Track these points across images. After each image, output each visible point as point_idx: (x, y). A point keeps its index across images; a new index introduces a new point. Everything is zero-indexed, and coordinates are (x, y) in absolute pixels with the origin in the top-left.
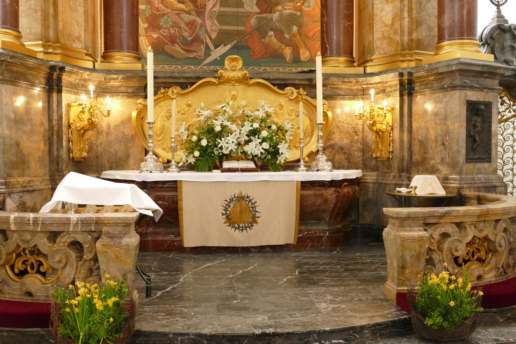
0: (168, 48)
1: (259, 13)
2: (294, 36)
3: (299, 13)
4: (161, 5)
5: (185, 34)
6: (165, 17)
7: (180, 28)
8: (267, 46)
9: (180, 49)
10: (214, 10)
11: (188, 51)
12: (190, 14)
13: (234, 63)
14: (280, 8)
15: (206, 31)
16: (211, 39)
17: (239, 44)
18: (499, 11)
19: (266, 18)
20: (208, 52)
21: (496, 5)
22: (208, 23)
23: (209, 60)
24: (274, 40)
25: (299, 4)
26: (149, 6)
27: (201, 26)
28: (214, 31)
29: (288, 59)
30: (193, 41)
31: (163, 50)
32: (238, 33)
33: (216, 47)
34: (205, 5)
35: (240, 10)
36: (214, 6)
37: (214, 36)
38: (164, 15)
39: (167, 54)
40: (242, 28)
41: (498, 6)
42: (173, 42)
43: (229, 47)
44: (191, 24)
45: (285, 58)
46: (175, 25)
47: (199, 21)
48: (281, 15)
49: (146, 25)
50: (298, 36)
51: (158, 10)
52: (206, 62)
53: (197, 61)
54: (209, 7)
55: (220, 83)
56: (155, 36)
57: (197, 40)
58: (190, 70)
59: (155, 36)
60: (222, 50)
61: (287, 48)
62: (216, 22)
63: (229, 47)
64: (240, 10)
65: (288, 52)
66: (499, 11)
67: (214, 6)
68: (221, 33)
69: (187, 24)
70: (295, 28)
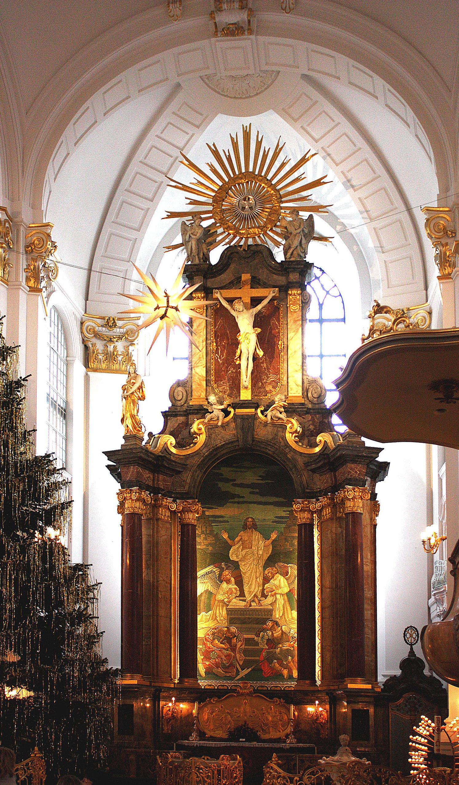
0: (215, 670)
1: (268, 649)
2: (289, 663)
3: (292, 649)
4: (211, 645)
5: (225, 662)
6: (213, 652)
7: (222, 659)
8: (273, 669)
9: (221, 671)
10: (241, 647)
11: (226, 672)
12: (227, 650)
13: (246, 685)
14: (281, 646)
15: (237, 660)
16: (239, 665)
17: (256, 668)
18: (412, 649)
19: (272, 652)
20: (238, 673)
21: (409, 645)
22: (238, 655)
23: (238, 677)
24: (277, 665)
25: (292, 643)
26: (204, 646)
27: (234, 657)
28: (241, 660)
29: (285, 677)
30: (229, 666)
31: (212, 671)
32: (256, 661)
33: (242, 670)
34: (236, 645)
35: (257, 647)
36: (241, 645)
37: (241, 663)
38: (213, 651)
39: (214, 674)
40: (258, 658)
41: (411, 645)
42: (218, 667)
43: (250, 669)
44: (227, 656)
45: (284, 677)
46: (219, 656)
47: (233, 654)
48: (281, 650)
49: (202, 657)
50: (292, 663)
51: (209, 648)
52: (236, 679)
53: (231, 678)
54: (238, 646)
55: (238, 696)
56: (207, 663)
57: (232, 665)
58: (228, 684)
59: (207, 663)
60: (246, 671)
61: (285, 670)
62: (242, 655)
63: (250, 669)
64: (257, 647)
65: (285, 672)
66: (412, 649)
67: (241, 645)
68: (245, 661)
69: (226, 656)
70: (290, 658)
